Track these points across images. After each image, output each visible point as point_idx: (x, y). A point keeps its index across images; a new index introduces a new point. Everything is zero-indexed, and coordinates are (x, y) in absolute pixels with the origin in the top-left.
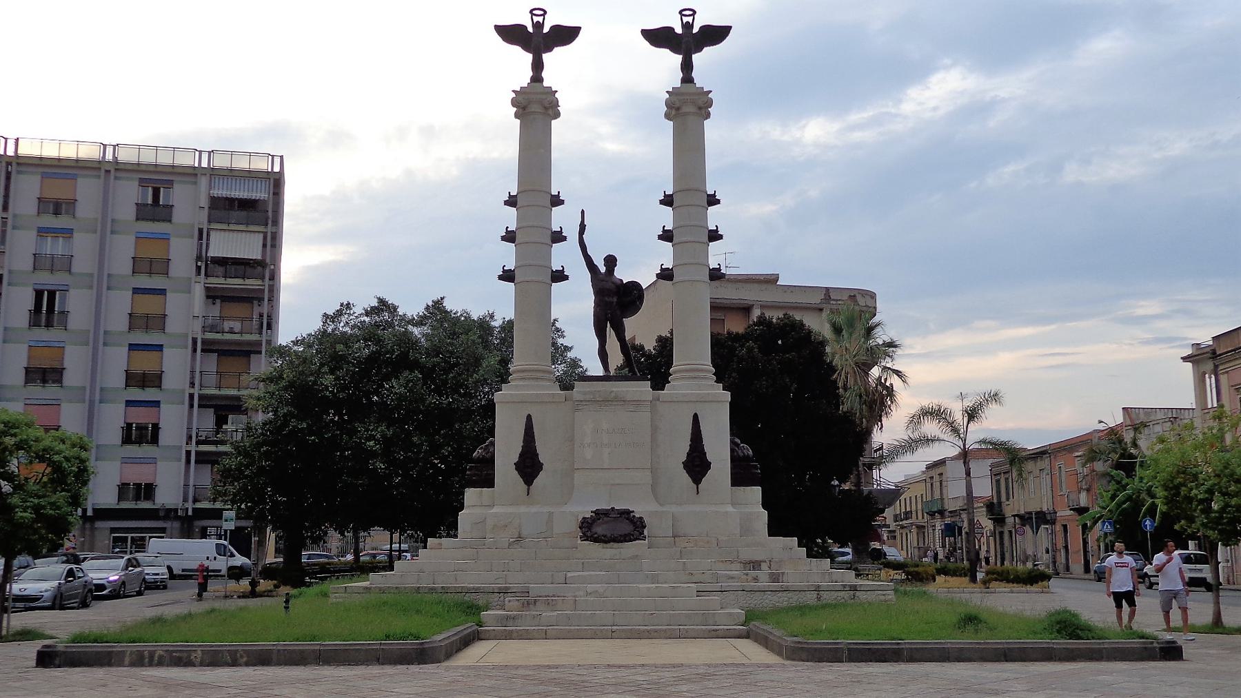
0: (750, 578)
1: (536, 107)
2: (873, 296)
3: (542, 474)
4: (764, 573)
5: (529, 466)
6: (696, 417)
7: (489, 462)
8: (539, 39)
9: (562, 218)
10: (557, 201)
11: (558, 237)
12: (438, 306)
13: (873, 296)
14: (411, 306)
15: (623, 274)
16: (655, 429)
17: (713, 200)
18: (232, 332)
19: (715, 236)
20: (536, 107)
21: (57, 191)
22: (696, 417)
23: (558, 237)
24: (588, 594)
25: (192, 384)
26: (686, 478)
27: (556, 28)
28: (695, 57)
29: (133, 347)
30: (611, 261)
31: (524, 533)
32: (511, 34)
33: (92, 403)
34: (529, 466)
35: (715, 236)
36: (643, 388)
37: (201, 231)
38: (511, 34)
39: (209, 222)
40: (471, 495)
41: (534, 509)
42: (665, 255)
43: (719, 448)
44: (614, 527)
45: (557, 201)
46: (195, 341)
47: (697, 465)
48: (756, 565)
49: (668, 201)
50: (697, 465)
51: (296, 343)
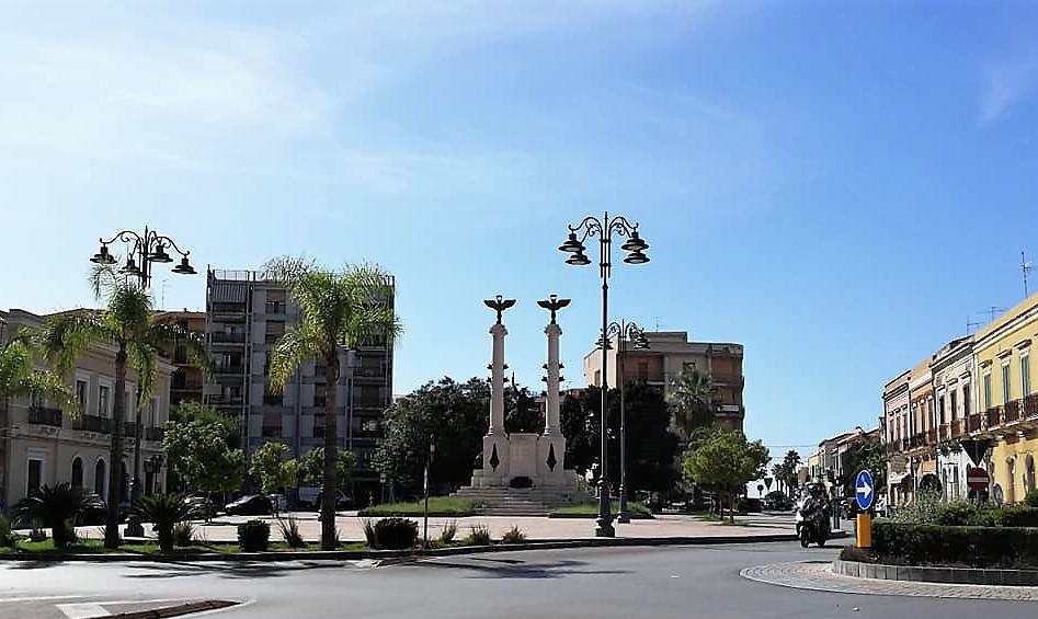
1: (499, 332)
2: (741, 347)
4: (567, 500)
5: (494, 461)
7: (481, 460)
8: (499, 306)
9: (507, 374)
10: (506, 367)
11: (506, 380)
12: (474, 380)
13: (741, 347)
14: (461, 379)
16: (537, 450)
17: (561, 366)
18: (369, 375)
19: (561, 379)
20: (499, 332)
21: (276, 297)
23: (506, 380)
25: (349, 405)
27: (506, 301)
28: (556, 312)
29: (317, 384)
32: (490, 304)
33: (298, 416)
34: (494, 461)
35: (561, 379)
38: (490, 304)
40: (475, 472)
42: (544, 387)
43: (560, 457)
44: (521, 482)
45: (506, 367)
46: (350, 380)
47: (552, 461)
48: (566, 496)
49: (545, 367)
50: (552, 461)
51: (408, 396)
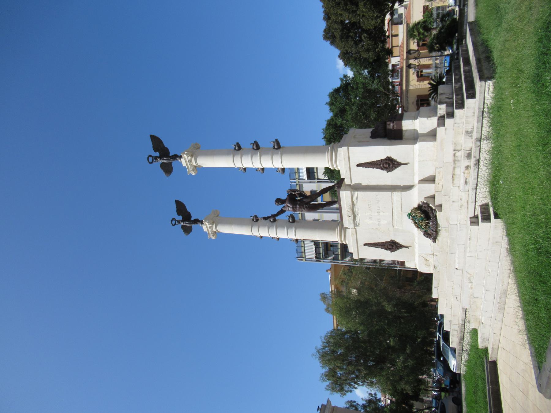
0: (467, 171)
3: (397, 240)
6: (359, 165)
15: (284, 196)
22: (359, 165)
24: (471, 282)
26: (397, 171)
30: (279, 201)
31: (431, 253)
34: (393, 246)
36: (345, 195)
37: (318, 182)
39: (315, 179)
41: (416, 246)
47: (389, 164)
50: (389, 164)
